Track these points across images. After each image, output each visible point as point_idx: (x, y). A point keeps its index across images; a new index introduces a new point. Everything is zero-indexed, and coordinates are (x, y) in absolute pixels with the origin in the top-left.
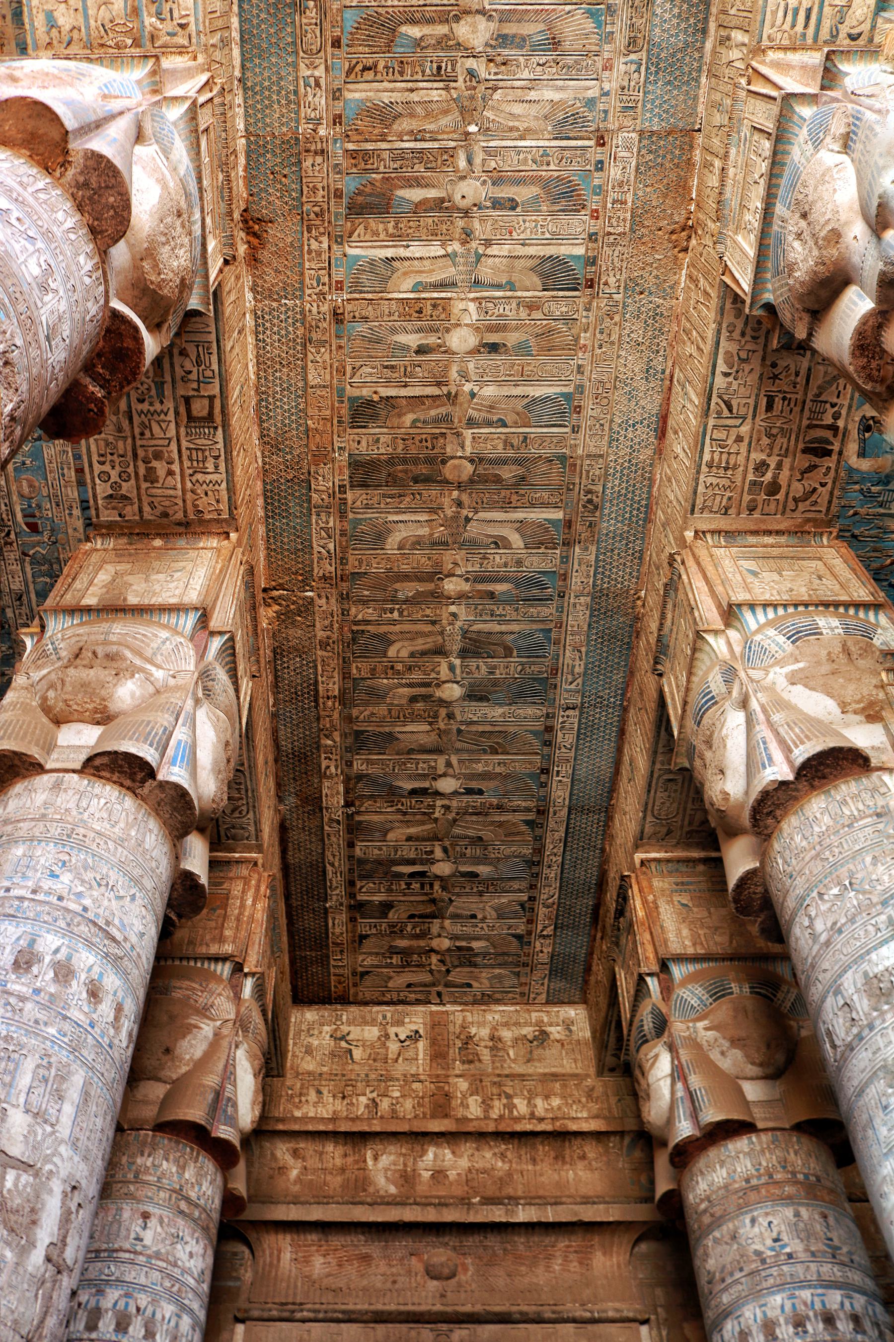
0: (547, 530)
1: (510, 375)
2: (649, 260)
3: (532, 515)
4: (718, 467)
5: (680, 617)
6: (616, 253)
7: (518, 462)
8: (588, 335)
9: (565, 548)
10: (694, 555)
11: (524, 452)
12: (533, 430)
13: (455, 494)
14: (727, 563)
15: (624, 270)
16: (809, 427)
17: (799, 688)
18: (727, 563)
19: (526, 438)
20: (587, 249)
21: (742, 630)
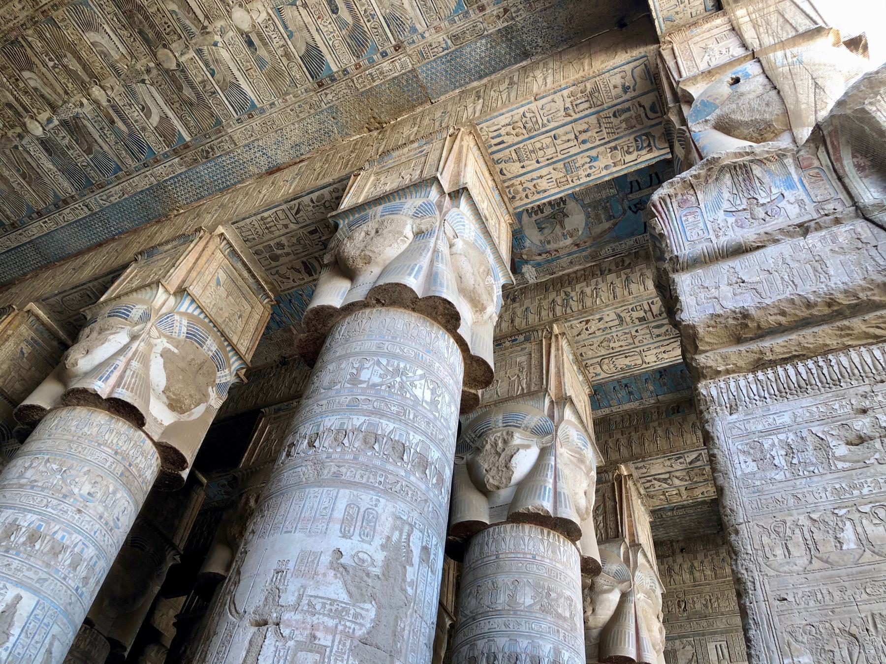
0: (174, 135)
1: (242, 63)
2: (353, 112)
3: (175, 122)
4: (265, 224)
5: (170, 256)
6: (345, 91)
7: (198, 95)
8: (293, 99)
9: (172, 152)
10: (208, 242)
11: (206, 96)
12: (222, 95)
13: (152, 65)
14: (215, 264)
15: (339, 101)
16: (316, 258)
17: (161, 361)
18: (215, 264)
19: (214, 93)
20: (337, 72)
21: (177, 304)
